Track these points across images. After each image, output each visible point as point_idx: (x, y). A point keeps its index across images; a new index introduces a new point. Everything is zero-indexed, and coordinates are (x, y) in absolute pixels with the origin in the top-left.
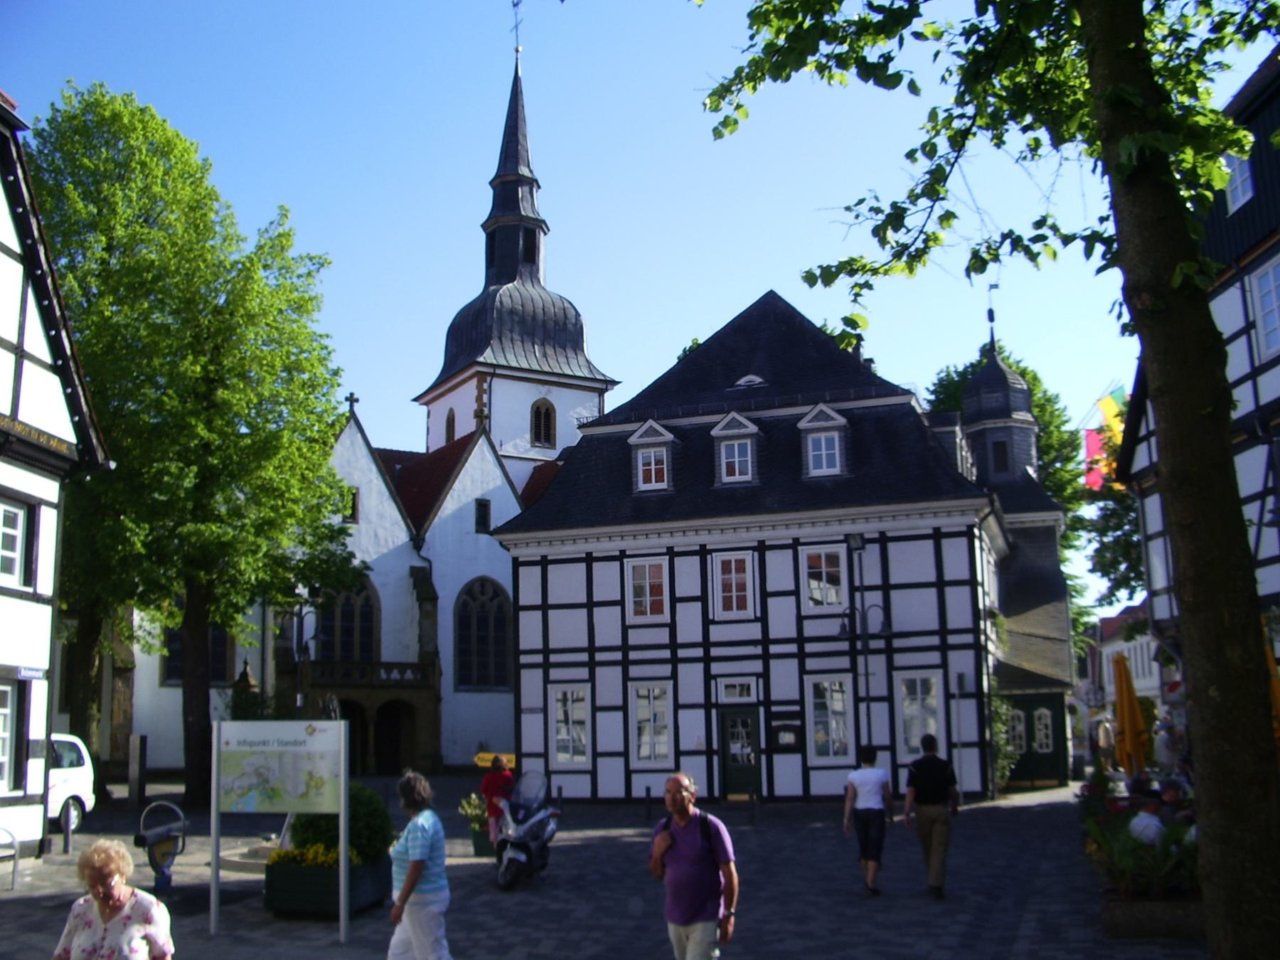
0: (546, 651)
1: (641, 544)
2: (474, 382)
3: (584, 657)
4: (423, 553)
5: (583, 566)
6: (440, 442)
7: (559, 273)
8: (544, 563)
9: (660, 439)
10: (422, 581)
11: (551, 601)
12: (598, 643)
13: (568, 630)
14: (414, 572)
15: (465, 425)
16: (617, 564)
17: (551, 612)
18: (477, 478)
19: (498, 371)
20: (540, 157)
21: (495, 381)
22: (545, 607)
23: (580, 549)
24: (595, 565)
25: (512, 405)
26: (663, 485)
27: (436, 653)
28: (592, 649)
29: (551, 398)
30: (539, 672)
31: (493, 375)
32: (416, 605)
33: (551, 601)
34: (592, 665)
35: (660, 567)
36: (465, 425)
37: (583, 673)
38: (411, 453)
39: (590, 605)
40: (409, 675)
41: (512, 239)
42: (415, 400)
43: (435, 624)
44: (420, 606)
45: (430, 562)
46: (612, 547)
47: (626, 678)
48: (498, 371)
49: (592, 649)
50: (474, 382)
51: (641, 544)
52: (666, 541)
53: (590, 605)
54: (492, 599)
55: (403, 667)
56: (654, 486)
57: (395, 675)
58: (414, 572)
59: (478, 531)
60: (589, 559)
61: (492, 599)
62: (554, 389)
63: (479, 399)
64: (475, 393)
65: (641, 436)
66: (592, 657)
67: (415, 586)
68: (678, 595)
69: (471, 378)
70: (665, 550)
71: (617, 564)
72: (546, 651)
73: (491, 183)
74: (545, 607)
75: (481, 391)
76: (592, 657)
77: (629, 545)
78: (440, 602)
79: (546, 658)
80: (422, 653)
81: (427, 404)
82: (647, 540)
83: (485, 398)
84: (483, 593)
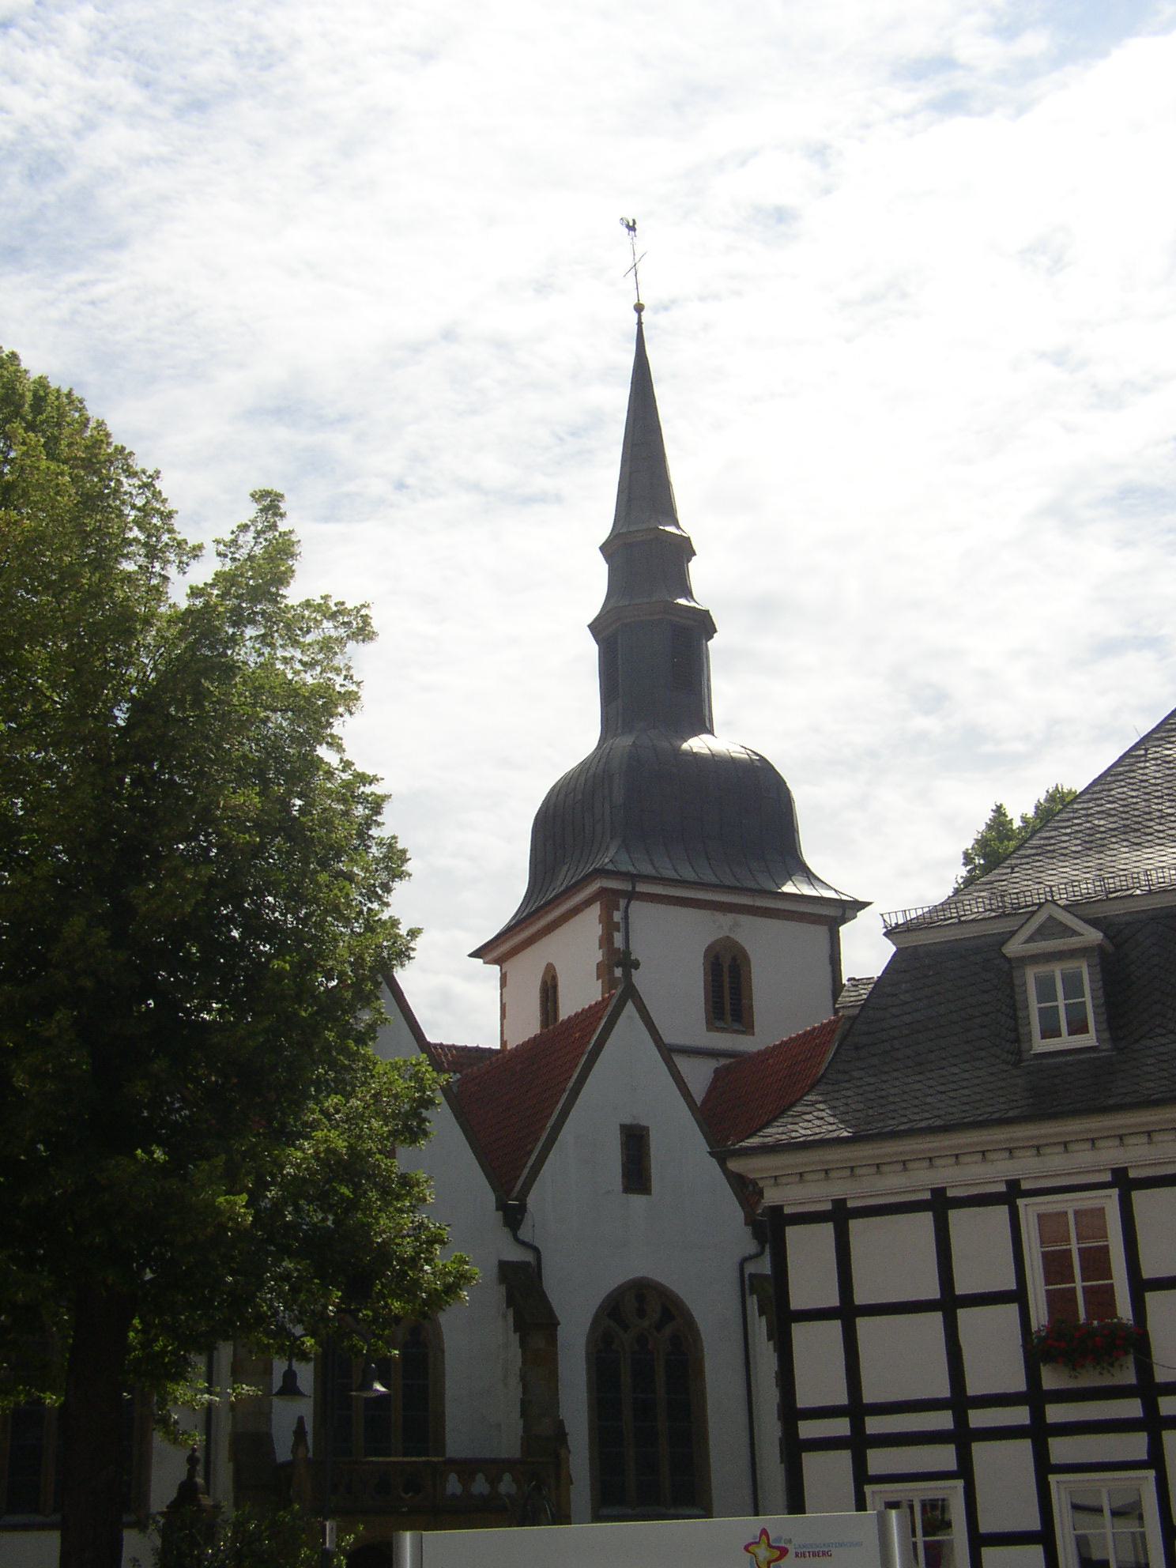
0: (856, 1409)
1: (1055, 1165)
2: (595, 910)
3: (943, 1420)
4: (524, 1233)
5: (926, 1219)
6: (529, 1027)
7: (739, 719)
8: (840, 1215)
9: (1073, 942)
10: (524, 1290)
11: (860, 1298)
12: (973, 1388)
13: (904, 1360)
14: (507, 1272)
15: (580, 992)
16: (1003, 1210)
17: (836, 1326)
18: (631, 1080)
19: (641, 888)
20: (694, 512)
21: (636, 906)
22: (847, 1312)
23: (920, 1181)
24: (954, 1215)
25: (672, 948)
26: (1089, 1039)
27: (560, 1435)
28: (959, 1401)
29: (742, 938)
30: (844, 1457)
31: (632, 896)
32: (515, 1338)
33: (860, 1298)
34: (962, 1438)
35: (1100, 1212)
36: (580, 992)
37: (944, 1457)
38: (477, 1050)
39: (949, 1303)
40: (507, 1485)
41: (653, 642)
42: (471, 955)
43: (553, 1376)
44: (523, 1343)
45: (536, 1250)
46: (991, 1175)
47: (1044, 1467)
48: (641, 888)
49: (959, 1401)
50: (595, 910)
51: (1055, 1165)
52: (1111, 1155)
53: (949, 1303)
54: (659, 1327)
55: (494, 1468)
56: (1066, 1041)
57: (480, 1486)
58: (507, 1272)
59: (628, 1189)
60: (940, 1204)
61: (659, 1327)
62: (744, 919)
63: (606, 941)
64: (598, 930)
65: (1030, 939)
66: (961, 1419)
67: (510, 1301)
68: (1147, 1274)
69: (587, 903)
70: (1107, 1177)
71: (1003, 1210)
72: (856, 1409)
73: (604, 549)
74: (847, 1312)
75: (609, 927)
76: (961, 1419)
77: (1026, 1168)
78: (562, 1332)
79: (858, 1426)
80: (529, 1439)
81: (498, 961)
82: (1067, 1157)
83: (618, 939)
84: (641, 1313)
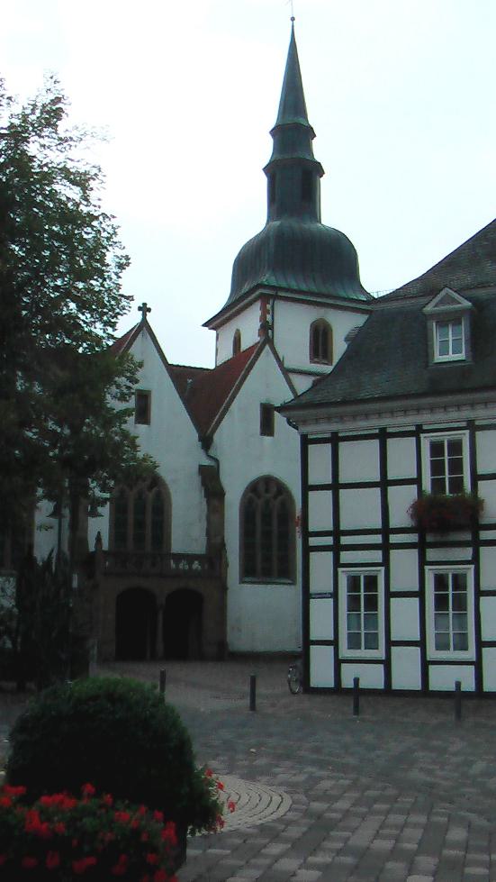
0: (337, 533)
2: (258, 305)
3: (378, 539)
4: (212, 452)
5: (376, 443)
10: (210, 480)
13: (361, 510)
18: (264, 385)
19: (281, 294)
20: (316, 114)
23: (375, 424)
24: (390, 441)
25: (294, 326)
26: (462, 356)
27: (223, 545)
28: (386, 530)
30: (330, 555)
31: (276, 297)
33: (343, 479)
34: (386, 547)
37: (377, 556)
40: (196, 565)
42: (205, 325)
45: (217, 461)
46: (409, 422)
48: (281, 294)
49: (386, 530)
50: (258, 305)
51: (439, 417)
53: (384, 483)
55: (190, 558)
56: (451, 357)
57: (183, 565)
63: (263, 318)
64: (259, 313)
65: (436, 306)
67: (204, 483)
72: (337, 533)
74: (335, 486)
75: (265, 312)
80: (209, 545)
84: (267, 491)
